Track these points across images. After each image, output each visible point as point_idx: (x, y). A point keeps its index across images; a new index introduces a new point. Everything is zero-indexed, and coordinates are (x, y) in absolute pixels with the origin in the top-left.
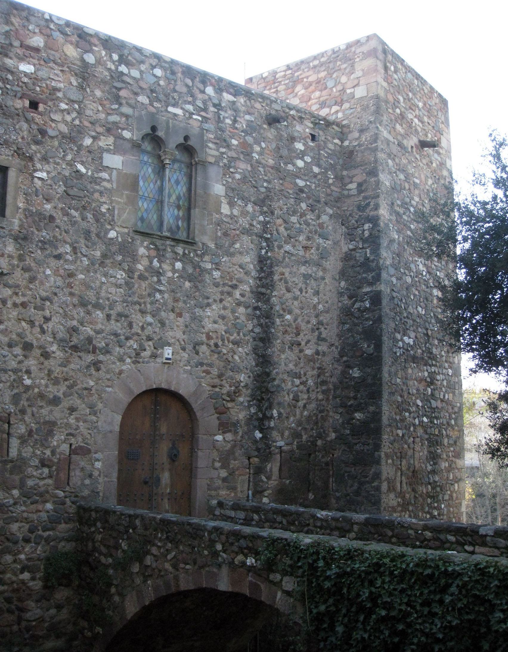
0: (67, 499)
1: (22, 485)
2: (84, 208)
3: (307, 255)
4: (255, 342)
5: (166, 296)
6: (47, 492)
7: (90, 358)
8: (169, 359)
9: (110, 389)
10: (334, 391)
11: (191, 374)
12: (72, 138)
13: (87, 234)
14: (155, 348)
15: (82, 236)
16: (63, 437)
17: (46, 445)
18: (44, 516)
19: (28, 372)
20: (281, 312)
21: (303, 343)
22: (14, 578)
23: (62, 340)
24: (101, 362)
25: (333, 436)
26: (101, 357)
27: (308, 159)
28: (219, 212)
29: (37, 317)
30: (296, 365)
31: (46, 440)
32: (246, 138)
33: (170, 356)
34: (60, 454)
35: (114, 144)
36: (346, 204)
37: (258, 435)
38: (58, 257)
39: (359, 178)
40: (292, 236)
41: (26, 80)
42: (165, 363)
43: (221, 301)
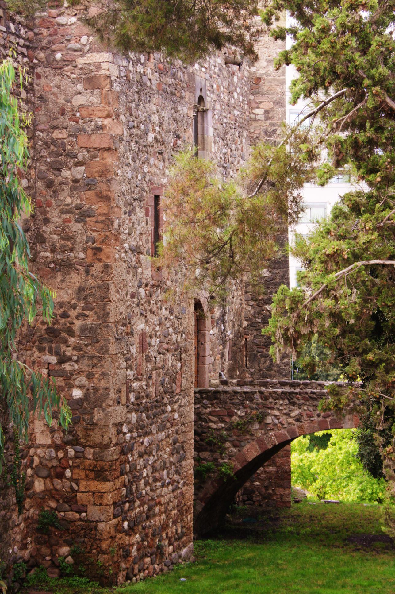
36: (253, 127)
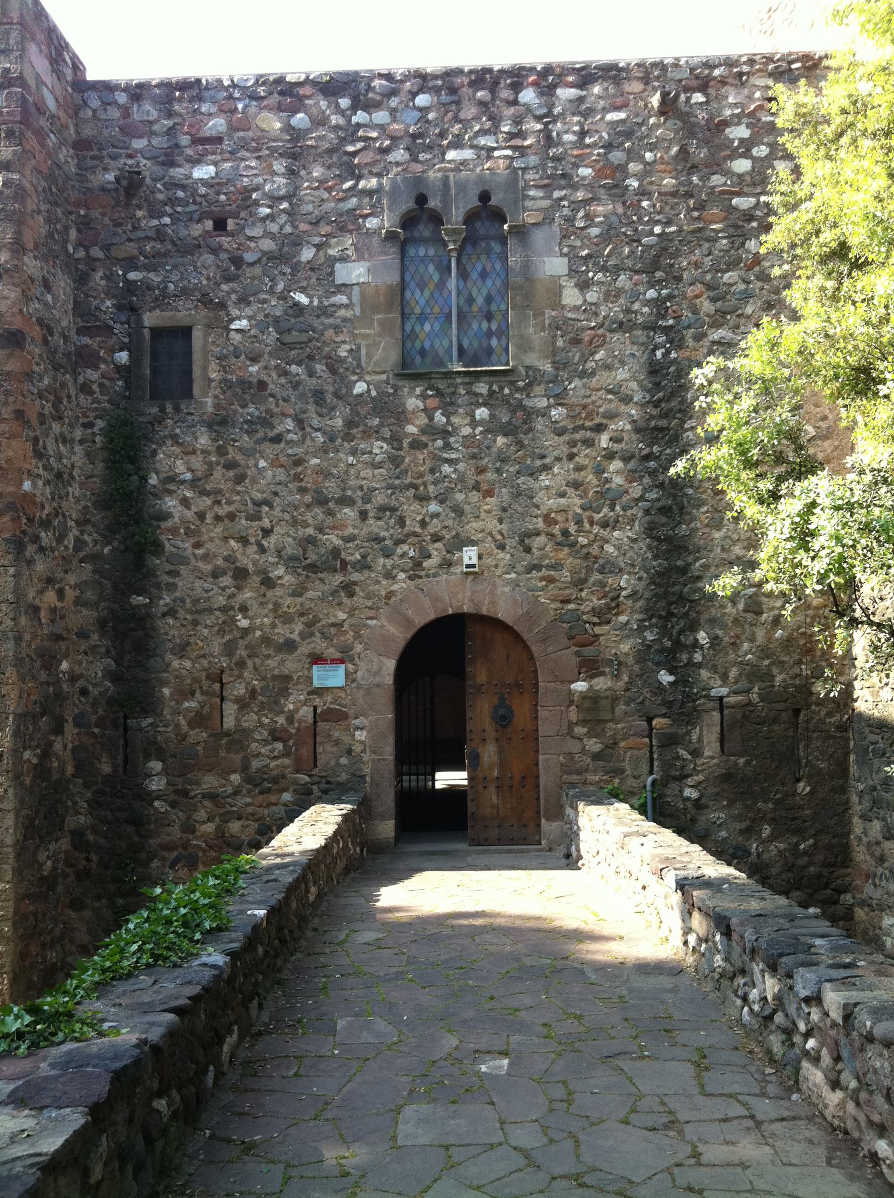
0: (315, 787)
1: (245, 768)
2: (311, 358)
5: (461, 466)
6: (284, 777)
7: (339, 578)
8: (473, 566)
9: (374, 622)
12: (283, 255)
13: (319, 396)
14: (448, 552)
15: (311, 400)
19: (244, 609)
23: (293, 558)
24: (355, 583)
26: (356, 576)
29: (251, 531)
31: (277, 702)
32: (610, 156)
33: (475, 561)
34: (300, 721)
37: (666, 678)
38: (277, 439)
40: (724, 309)
41: (202, 190)
42: (467, 574)
43: (571, 457)
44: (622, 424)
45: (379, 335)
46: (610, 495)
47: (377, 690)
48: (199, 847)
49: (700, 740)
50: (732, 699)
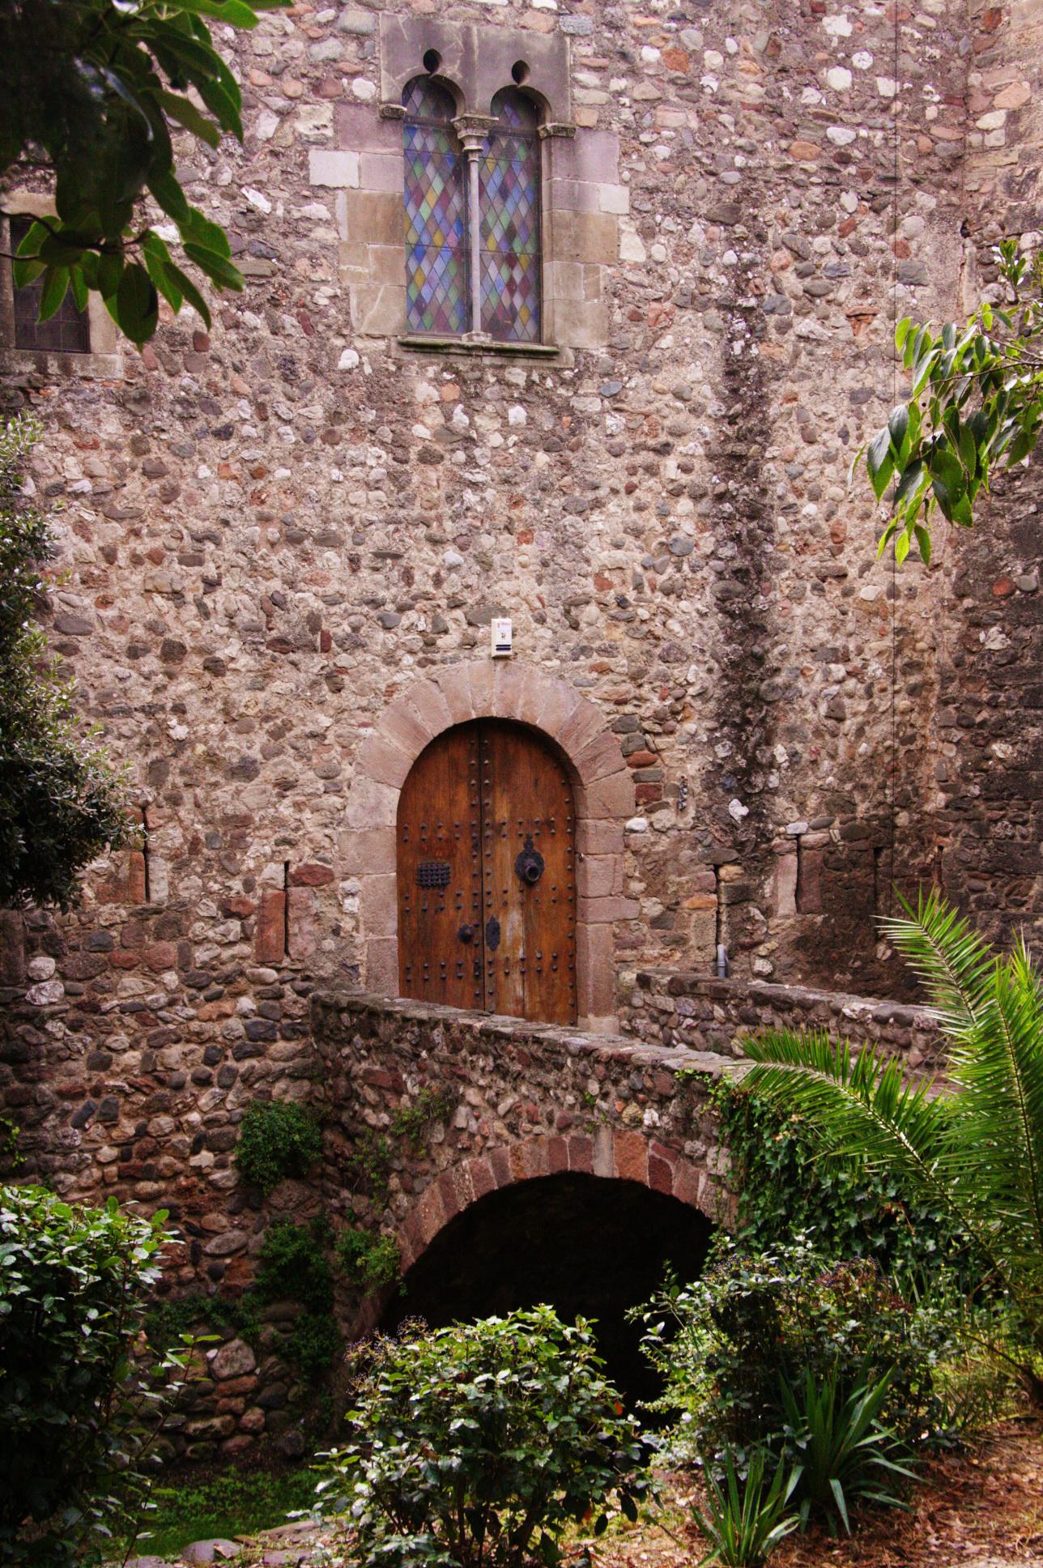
0: (287, 987)
1: (184, 962)
2: (274, 302)
3: (861, 338)
4: (722, 584)
5: (490, 494)
6: (242, 973)
9: (369, 731)
10: (943, 688)
11: (561, 677)
14: (470, 624)
15: (277, 373)
16: (268, 850)
17: (232, 869)
18: (236, 1025)
19: (179, 710)
20: (791, 499)
21: (853, 572)
22: (180, 1166)
23: (252, 629)
24: (343, 670)
25: (939, 799)
26: (344, 660)
27: (863, 60)
28: (614, 260)
29: (187, 583)
30: (834, 630)
33: (508, 641)
34: (266, 885)
35: (334, 121)
36: (975, 175)
37: (738, 810)
38: (225, 433)
39: (1009, 99)
40: (815, 291)
42: (496, 658)
43: (630, 490)
44: (691, 447)
45: (375, 277)
46: (676, 550)
47: (374, 836)
48: (121, 1090)
49: (774, 894)
50: (812, 838)
